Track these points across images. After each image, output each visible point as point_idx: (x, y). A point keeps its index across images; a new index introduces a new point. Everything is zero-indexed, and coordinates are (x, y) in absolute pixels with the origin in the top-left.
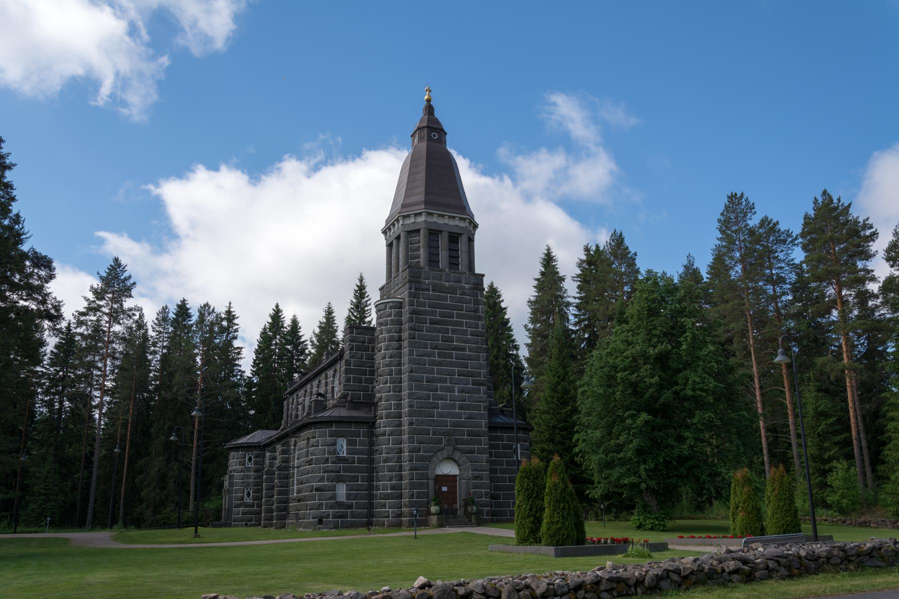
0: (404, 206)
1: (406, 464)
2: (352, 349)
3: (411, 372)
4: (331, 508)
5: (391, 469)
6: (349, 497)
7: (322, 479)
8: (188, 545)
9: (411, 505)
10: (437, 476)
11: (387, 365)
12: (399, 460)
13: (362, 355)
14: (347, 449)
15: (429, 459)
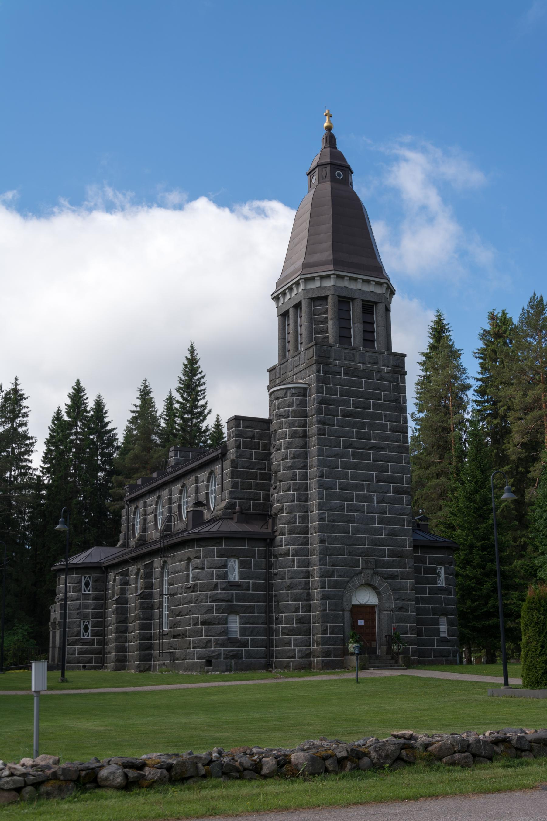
0: (305, 266)
1: (316, 592)
2: (238, 447)
3: (321, 476)
4: (222, 645)
5: (296, 598)
6: (243, 632)
7: (209, 610)
8: (87, 691)
9: (325, 641)
10: (354, 606)
11: (290, 468)
12: (307, 586)
13: (251, 454)
14: (240, 572)
15: (343, 585)
